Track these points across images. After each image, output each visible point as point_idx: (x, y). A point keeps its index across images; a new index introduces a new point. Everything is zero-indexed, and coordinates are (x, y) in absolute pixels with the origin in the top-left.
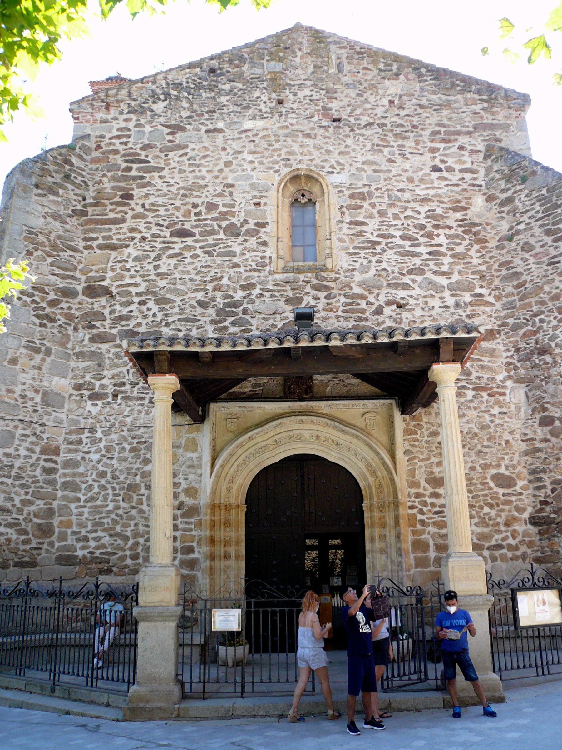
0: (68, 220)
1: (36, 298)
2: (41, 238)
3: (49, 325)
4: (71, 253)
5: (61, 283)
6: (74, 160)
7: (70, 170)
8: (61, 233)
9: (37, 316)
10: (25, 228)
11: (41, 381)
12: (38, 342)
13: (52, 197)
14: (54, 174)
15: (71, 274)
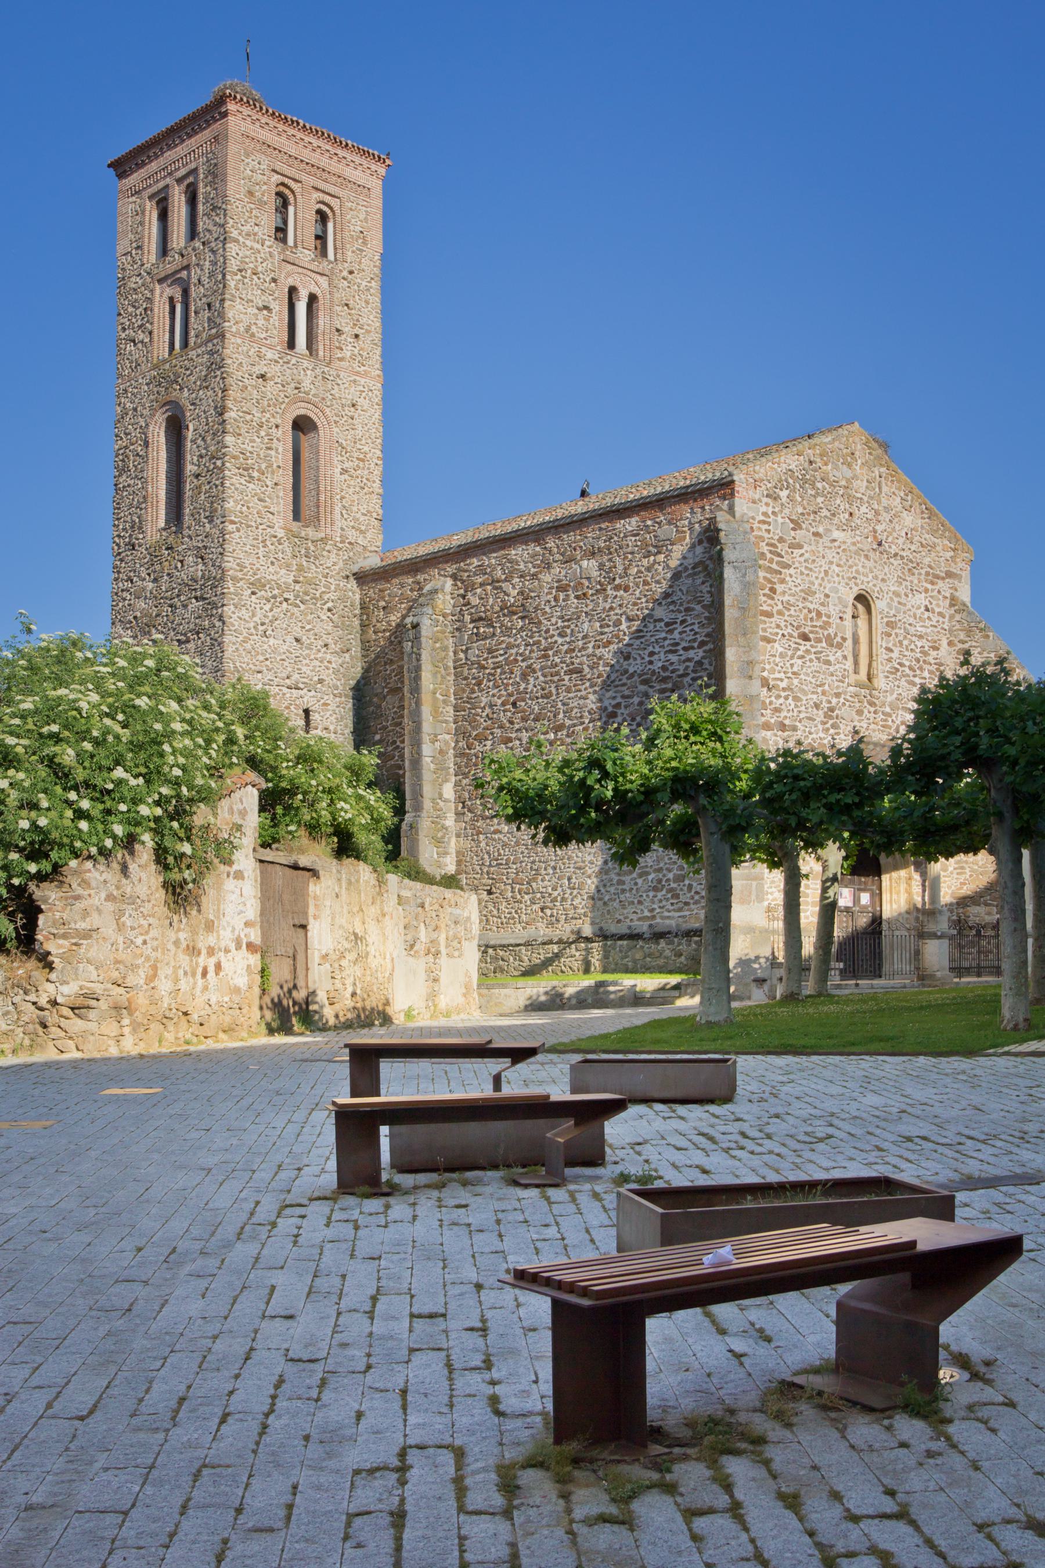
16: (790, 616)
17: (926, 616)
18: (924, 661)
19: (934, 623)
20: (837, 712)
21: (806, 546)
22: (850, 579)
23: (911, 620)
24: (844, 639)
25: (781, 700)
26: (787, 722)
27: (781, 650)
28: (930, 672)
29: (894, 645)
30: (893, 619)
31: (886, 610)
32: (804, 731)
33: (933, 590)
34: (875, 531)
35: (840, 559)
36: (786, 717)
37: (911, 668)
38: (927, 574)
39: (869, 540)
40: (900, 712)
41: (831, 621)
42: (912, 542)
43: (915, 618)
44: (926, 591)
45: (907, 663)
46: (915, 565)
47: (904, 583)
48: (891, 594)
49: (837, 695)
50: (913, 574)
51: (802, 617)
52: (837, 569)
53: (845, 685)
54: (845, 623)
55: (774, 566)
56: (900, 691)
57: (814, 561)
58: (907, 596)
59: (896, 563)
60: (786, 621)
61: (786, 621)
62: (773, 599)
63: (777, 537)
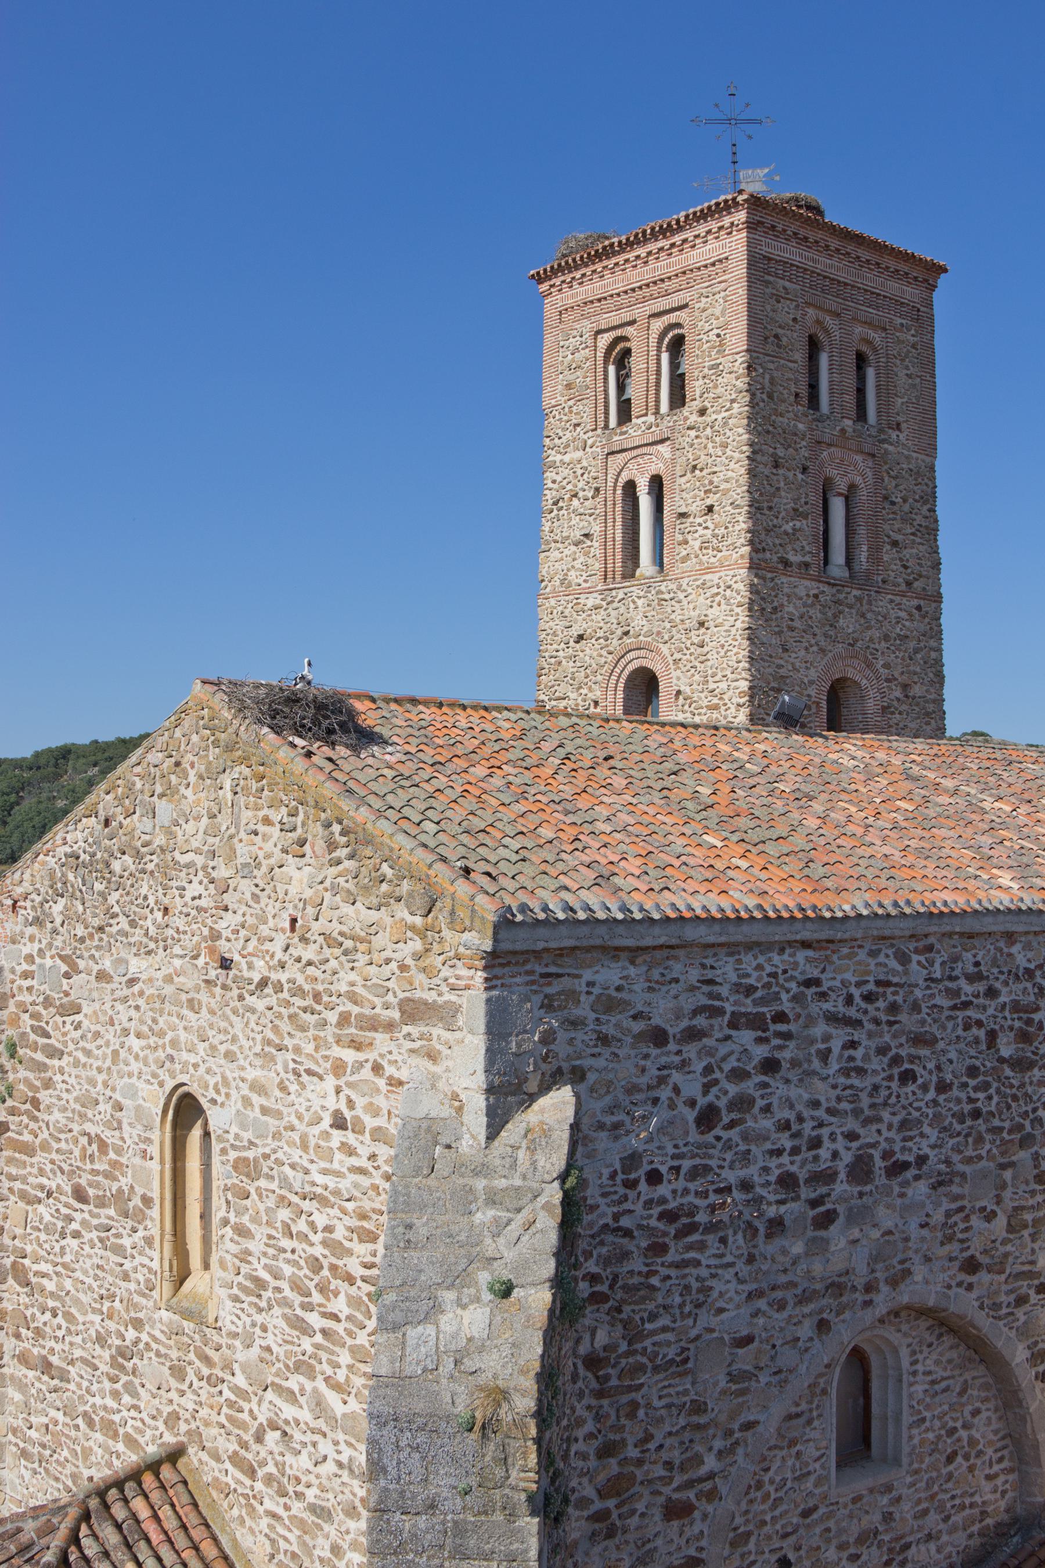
16: (58, 1151)
17: (335, 1143)
18: (333, 1268)
19: (363, 1162)
20: (135, 1360)
21: (85, 1009)
23: (296, 1155)
24: (147, 1201)
26: (55, 1360)
27: (47, 1218)
28: (354, 1302)
29: (255, 1220)
30: (250, 1154)
31: (234, 1129)
32: (79, 1386)
33: (360, 1065)
34: (215, 936)
35: (142, 1022)
37: (297, 1286)
38: (344, 1019)
39: (201, 962)
40: (270, 1395)
42: (304, 939)
43: (305, 1147)
44: (339, 1068)
45: (288, 1270)
46: (309, 1002)
47: (280, 1057)
48: (245, 1091)
49: (138, 1324)
51: (77, 1152)
53: (151, 1304)
55: (39, 1056)
57: (97, 1035)
59: (260, 1005)
60: (52, 1162)
61: (52, 1162)
62: (35, 1119)
63: (41, 999)
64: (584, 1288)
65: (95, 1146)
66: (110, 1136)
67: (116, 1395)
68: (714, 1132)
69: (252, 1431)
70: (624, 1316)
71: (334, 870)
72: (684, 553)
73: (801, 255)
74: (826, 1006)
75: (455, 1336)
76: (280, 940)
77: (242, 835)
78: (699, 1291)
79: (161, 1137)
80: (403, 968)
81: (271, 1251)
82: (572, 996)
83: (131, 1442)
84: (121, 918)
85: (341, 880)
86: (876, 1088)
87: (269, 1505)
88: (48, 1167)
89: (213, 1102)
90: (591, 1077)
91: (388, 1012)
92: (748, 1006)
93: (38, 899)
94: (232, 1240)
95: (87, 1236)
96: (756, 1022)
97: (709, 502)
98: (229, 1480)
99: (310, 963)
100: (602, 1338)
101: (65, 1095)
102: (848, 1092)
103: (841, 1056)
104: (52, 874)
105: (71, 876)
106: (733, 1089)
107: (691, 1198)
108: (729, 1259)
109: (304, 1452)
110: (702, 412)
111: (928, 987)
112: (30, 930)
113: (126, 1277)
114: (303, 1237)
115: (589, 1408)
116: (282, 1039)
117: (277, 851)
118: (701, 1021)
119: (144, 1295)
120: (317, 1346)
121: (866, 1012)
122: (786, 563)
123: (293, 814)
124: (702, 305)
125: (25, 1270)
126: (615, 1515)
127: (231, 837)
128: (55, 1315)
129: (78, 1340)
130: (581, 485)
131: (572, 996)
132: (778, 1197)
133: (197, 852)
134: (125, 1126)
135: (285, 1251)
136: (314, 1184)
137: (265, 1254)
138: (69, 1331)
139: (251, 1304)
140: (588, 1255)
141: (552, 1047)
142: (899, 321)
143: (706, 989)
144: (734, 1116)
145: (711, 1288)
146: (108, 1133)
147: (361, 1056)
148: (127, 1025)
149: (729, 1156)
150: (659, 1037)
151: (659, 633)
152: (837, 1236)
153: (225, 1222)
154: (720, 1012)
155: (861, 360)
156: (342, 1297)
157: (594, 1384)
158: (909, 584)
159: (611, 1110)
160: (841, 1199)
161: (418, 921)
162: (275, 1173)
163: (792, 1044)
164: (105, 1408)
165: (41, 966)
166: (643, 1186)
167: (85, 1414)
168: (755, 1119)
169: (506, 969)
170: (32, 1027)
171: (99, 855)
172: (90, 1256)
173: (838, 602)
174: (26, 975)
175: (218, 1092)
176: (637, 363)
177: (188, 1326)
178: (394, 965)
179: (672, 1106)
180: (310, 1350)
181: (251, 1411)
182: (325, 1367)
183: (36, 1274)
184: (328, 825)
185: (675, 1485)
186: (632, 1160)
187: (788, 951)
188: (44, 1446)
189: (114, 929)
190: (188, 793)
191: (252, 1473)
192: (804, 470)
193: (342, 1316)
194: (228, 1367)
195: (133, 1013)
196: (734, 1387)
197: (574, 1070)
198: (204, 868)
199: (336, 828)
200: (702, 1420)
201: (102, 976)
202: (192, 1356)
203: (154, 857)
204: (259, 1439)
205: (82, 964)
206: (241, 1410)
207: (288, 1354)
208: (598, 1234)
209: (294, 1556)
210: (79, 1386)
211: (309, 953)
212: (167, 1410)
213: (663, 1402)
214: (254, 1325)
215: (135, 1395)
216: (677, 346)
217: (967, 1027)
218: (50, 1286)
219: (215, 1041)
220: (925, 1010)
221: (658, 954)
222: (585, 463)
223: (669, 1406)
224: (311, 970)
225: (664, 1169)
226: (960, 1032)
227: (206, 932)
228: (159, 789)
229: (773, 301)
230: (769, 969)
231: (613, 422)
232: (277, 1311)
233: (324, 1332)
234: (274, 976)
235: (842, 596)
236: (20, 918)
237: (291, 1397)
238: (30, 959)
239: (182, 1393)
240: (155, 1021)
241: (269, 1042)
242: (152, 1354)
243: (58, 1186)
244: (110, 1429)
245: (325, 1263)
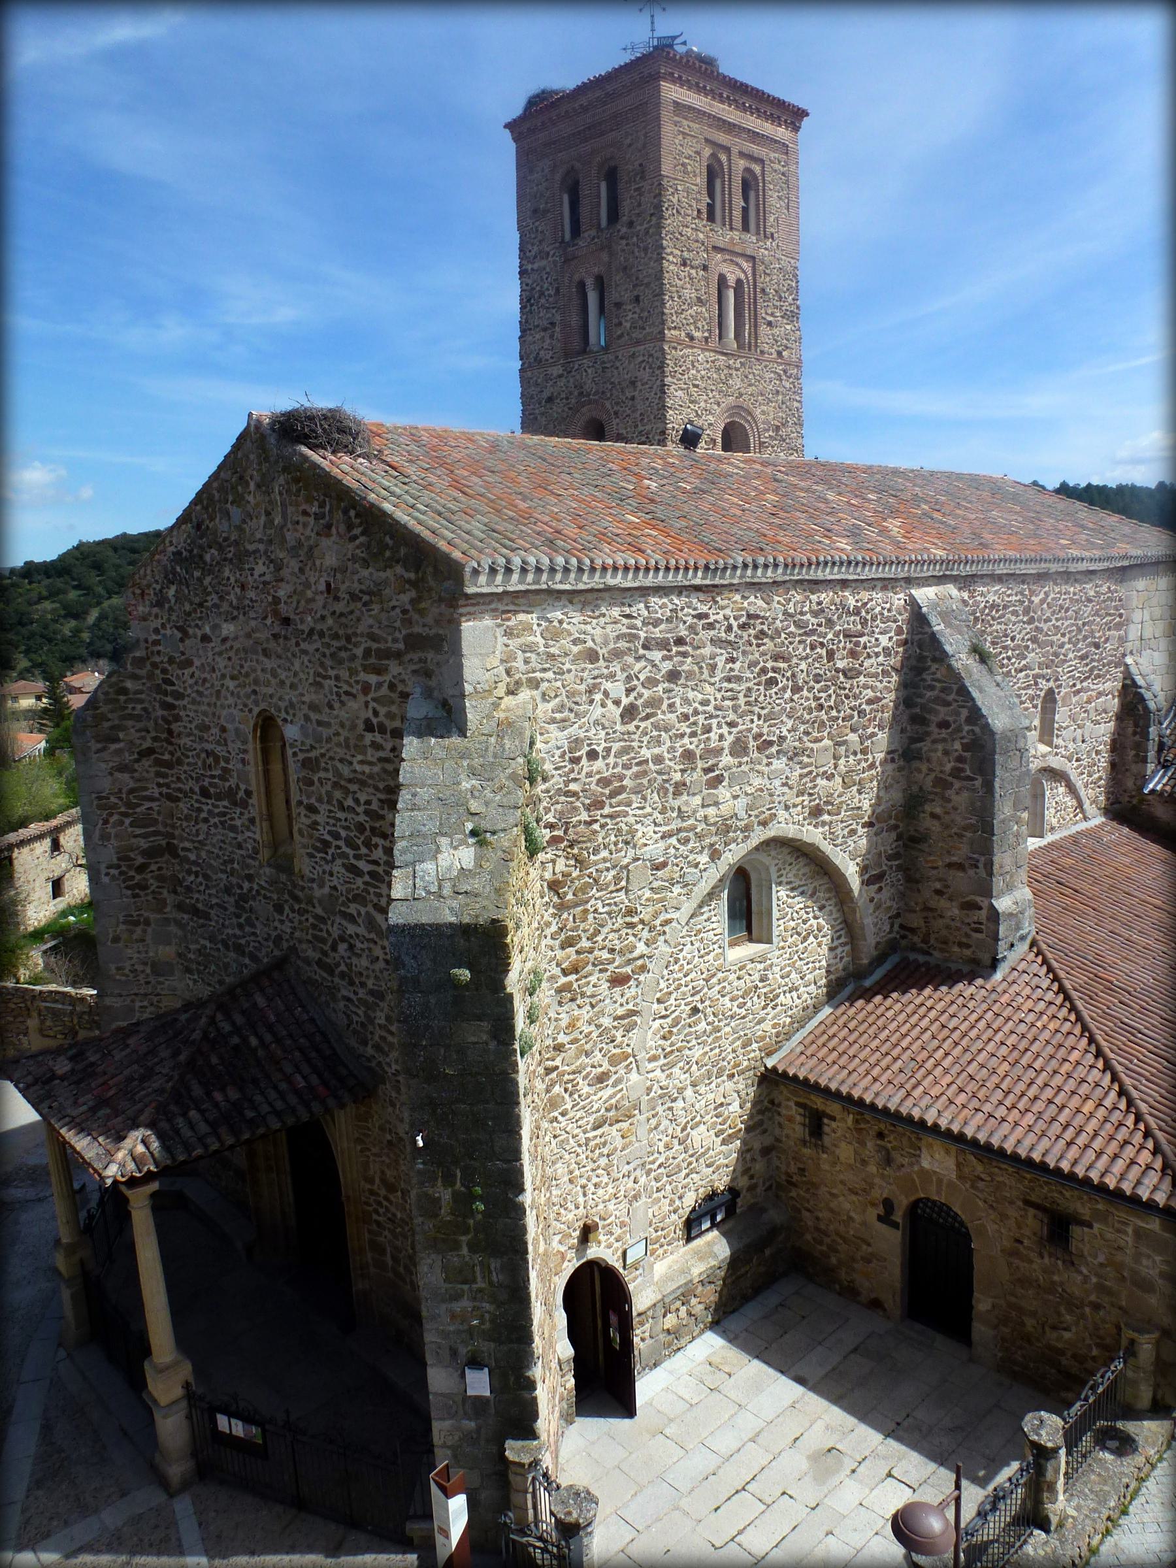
0: (136, 766)
1: (124, 868)
2: (113, 799)
3: (142, 893)
4: (147, 805)
5: (143, 844)
6: (129, 684)
7: (125, 702)
8: (132, 785)
9: (127, 888)
10: (94, 796)
11: (146, 952)
12: (135, 914)
13: (114, 747)
14: (110, 716)
15: (152, 829)
18: (373, 829)
20: (251, 902)
21: (197, 663)
22: (248, 696)
23: (341, 752)
24: (248, 793)
25: (192, 878)
26: (200, 906)
27: (186, 811)
29: (320, 800)
30: (313, 754)
34: (276, 601)
35: (233, 668)
36: (198, 899)
37: (350, 843)
38: (367, 653)
39: (269, 622)
40: (338, 919)
41: (230, 766)
42: (337, 598)
43: (348, 747)
44: (366, 688)
45: (343, 833)
46: (343, 642)
49: (250, 878)
50: (341, 662)
51: (200, 763)
52: (231, 684)
53: (257, 863)
54: (248, 768)
55: (169, 699)
56: (335, 882)
58: (331, 707)
59: (310, 647)
60: (185, 772)
61: (185, 772)
62: (171, 743)
63: (166, 659)
64: (546, 834)
65: (211, 759)
66: (220, 750)
67: (240, 926)
68: (635, 723)
69: (329, 944)
70: (576, 851)
71: (351, 546)
72: (619, 332)
73: (701, 101)
74: (712, 633)
75: (449, 869)
76: (320, 600)
77: (289, 525)
78: (628, 833)
79: (253, 748)
80: (405, 612)
81: (332, 821)
82: (528, 628)
83: (254, 958)
84: (214, 596)
85: (358, 551)
86: (749, 690)
87: (344, 992)
88: (183, 777)
89: (285, 720)
90: (545, 685)
91: (396, 646)
92: (657, 633)
93: (158, 587)
94: (305, 816)
95: (212, 821)
96: (663, 645)
97: (635, 293)
98: (317, 977)
99: (342, 615)
100: (561, 865)
101: (188, 725)
102: (729, 693)
103: (724, 667)
104: (165, 567)
105: (178, 569)
106: (646, 693)
107: (619, 770)
108: (648, 810)
109: (364, 955)
110: (631, 224)
111: (786, 620)
112: (155, 610)
113: (240, 847)
114: (351, 809)
115: (554, 915)
116: (326, 670)
117: (313, 535)
118: (622, 645)
119: (253, 858)
120: (366, 883)
121: (741, 637)
122: (692, 338)
123: (322, 505)
124: (628, 141)
125: (175, 847)
126: (575, 986)
127: (282, 528)
128: (197, 876)
129: (213, 891)
130: (546, 286)
131: (528, 628)
132: (682, 767)
133: (261, 541)
134: (229, 743)
135: (340, 820)
136: (355, 771)
137: (328, 823)
138: (207, 887)
139: (322, 858)
140: (547, 810)
141: (514, 664)
142: (773, 155)
143: (625, 621)
144: (648, 710)
145: (637, 830)
146: (219, 748)
147: (381, 679)
148: (223, 671)
149: (646, 739)
150: (592, 656)
151: (603, 393)
152: (723, 793)
153: (300, 803)
154: (637, 637)
155: (746, 186)
156: (380, 849)
157: (555, 899)
158: (779, 354)
159: (561, 708)
160: (729, 768)
161: (412, 576)
162: (329, 766)
163: (689, 660)
164: (234, 935)
165: (164, 635)
166: (584, 761)
167: (223, 940)
168: (664, 713)
169: (476, 608)
170: (163, 679)
171: (195, 551)
172: (215, 834)
173: (729, 367)
174: (156, 643)
175: (287, 713)
176: (585, 191)
177: (283, 877)
178: (398, 610)
179: (603, 705)
180: (362, 887)
181: (328, 931)
182: (372, 896)
183: (184, 849)
184: (346, 512)
185: (616, 964)
186: (576, 743)
187: (684, 593)
188: (199, 964)
189: (209, 604)
190: (251, 498)
191: (331, 972)
192: (705, 268)
193: (381, 862)
194: (310, 901)
195: (226, 662)
196: (656, 897)
197: (530, 680)
198: (266, 552)
199: (352, 513)
200: (635, 920)
201: (205, 639)
202: (286, 897)
203: (232, 549)
204: (334, 948)
205: (191, 631)
206: (321, 930)
207: (349, 891)
208: (554, 795)
209: (362, 1024)
210: (217, 922)
211: (340, 607)
212: (274, 934)
213: (606, 909)
214: (324, 872)
215: (253, 926)
216: (612, 176)
217: (813, 648)
218: (193, 857)
219: (283, 677)
220: (783, 636)
221: (589, 596)
222: (548, 270)
223: (609, 913)
224: (343, 620)
225: (599, 749)
226: (808, 651)
227: (270, 599)
228: (230, 498)
229: (680, 137)
230: (671, 606)
231: (568, 236)
232: (339, 862)
233: (369, 873)
234: (319, 627)
235: (731, 362)
236: (147, 603)
237: (352, 919)
238: (156, 631)
239: (282, 922)
240: (242, 666)
241: (319, 675)
242: (261, 898)
243: (191, 789)
244: (239, 949)
245: (367, 826)
